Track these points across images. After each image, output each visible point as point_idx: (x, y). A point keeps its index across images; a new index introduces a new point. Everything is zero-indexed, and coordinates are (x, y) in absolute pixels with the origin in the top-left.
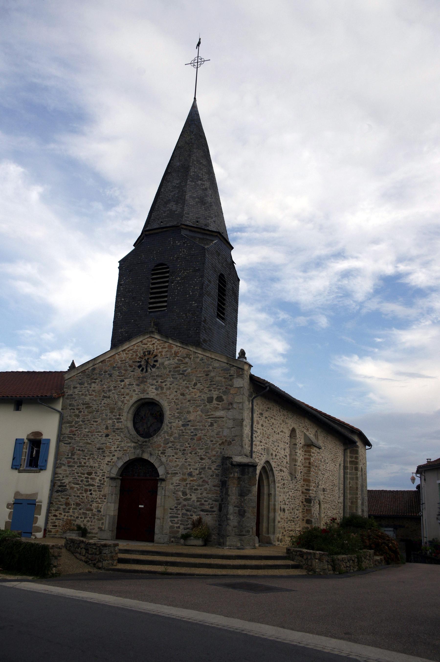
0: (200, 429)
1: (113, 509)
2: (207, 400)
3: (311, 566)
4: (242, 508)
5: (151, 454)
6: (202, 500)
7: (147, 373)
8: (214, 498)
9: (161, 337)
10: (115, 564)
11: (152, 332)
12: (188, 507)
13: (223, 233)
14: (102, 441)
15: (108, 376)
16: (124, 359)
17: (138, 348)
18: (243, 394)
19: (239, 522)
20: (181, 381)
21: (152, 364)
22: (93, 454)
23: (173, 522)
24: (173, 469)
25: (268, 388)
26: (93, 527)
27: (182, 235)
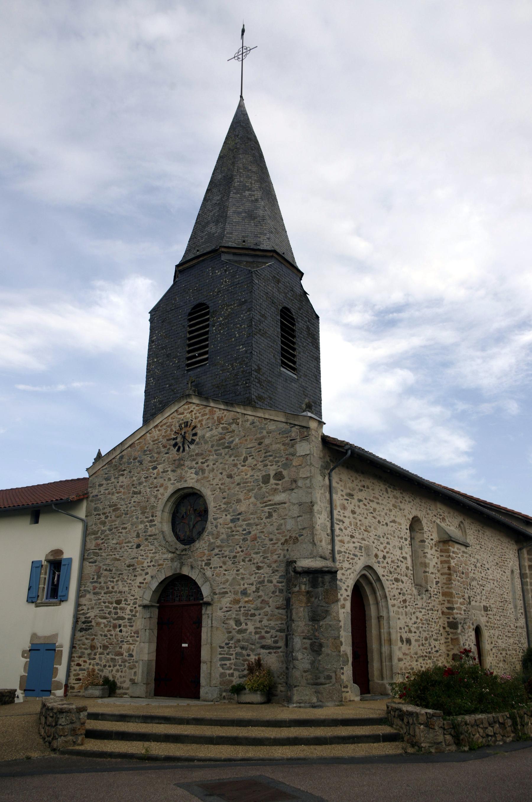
0: (255, 523)
1: (147, 652)
2: (261, 481)
3: (414, 736)
4: (315, 641)
5: (192, 567)
6: (262, 631)
7: (184, 453)
8: (279, 627)
9: (200, 400)
10: (79, 741)
11: (189, 396)
12: (243, 643)
13: (284, 253)
14: (133, 555)
15: (137, 464)
16: (156, 438)
17: (174, 420)
18: (311, 464)
19: (312, 663)
20: (227, 457)
21: (190, 440)
22: (122, 574)
23: (225, 666)
24: (222, 586)
25: (349, 452)
26: (124, 679)
27: (223, 261)
